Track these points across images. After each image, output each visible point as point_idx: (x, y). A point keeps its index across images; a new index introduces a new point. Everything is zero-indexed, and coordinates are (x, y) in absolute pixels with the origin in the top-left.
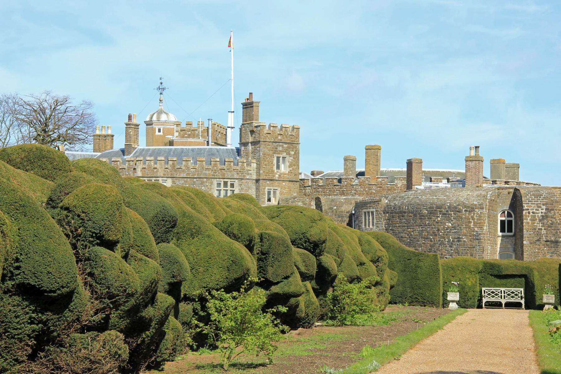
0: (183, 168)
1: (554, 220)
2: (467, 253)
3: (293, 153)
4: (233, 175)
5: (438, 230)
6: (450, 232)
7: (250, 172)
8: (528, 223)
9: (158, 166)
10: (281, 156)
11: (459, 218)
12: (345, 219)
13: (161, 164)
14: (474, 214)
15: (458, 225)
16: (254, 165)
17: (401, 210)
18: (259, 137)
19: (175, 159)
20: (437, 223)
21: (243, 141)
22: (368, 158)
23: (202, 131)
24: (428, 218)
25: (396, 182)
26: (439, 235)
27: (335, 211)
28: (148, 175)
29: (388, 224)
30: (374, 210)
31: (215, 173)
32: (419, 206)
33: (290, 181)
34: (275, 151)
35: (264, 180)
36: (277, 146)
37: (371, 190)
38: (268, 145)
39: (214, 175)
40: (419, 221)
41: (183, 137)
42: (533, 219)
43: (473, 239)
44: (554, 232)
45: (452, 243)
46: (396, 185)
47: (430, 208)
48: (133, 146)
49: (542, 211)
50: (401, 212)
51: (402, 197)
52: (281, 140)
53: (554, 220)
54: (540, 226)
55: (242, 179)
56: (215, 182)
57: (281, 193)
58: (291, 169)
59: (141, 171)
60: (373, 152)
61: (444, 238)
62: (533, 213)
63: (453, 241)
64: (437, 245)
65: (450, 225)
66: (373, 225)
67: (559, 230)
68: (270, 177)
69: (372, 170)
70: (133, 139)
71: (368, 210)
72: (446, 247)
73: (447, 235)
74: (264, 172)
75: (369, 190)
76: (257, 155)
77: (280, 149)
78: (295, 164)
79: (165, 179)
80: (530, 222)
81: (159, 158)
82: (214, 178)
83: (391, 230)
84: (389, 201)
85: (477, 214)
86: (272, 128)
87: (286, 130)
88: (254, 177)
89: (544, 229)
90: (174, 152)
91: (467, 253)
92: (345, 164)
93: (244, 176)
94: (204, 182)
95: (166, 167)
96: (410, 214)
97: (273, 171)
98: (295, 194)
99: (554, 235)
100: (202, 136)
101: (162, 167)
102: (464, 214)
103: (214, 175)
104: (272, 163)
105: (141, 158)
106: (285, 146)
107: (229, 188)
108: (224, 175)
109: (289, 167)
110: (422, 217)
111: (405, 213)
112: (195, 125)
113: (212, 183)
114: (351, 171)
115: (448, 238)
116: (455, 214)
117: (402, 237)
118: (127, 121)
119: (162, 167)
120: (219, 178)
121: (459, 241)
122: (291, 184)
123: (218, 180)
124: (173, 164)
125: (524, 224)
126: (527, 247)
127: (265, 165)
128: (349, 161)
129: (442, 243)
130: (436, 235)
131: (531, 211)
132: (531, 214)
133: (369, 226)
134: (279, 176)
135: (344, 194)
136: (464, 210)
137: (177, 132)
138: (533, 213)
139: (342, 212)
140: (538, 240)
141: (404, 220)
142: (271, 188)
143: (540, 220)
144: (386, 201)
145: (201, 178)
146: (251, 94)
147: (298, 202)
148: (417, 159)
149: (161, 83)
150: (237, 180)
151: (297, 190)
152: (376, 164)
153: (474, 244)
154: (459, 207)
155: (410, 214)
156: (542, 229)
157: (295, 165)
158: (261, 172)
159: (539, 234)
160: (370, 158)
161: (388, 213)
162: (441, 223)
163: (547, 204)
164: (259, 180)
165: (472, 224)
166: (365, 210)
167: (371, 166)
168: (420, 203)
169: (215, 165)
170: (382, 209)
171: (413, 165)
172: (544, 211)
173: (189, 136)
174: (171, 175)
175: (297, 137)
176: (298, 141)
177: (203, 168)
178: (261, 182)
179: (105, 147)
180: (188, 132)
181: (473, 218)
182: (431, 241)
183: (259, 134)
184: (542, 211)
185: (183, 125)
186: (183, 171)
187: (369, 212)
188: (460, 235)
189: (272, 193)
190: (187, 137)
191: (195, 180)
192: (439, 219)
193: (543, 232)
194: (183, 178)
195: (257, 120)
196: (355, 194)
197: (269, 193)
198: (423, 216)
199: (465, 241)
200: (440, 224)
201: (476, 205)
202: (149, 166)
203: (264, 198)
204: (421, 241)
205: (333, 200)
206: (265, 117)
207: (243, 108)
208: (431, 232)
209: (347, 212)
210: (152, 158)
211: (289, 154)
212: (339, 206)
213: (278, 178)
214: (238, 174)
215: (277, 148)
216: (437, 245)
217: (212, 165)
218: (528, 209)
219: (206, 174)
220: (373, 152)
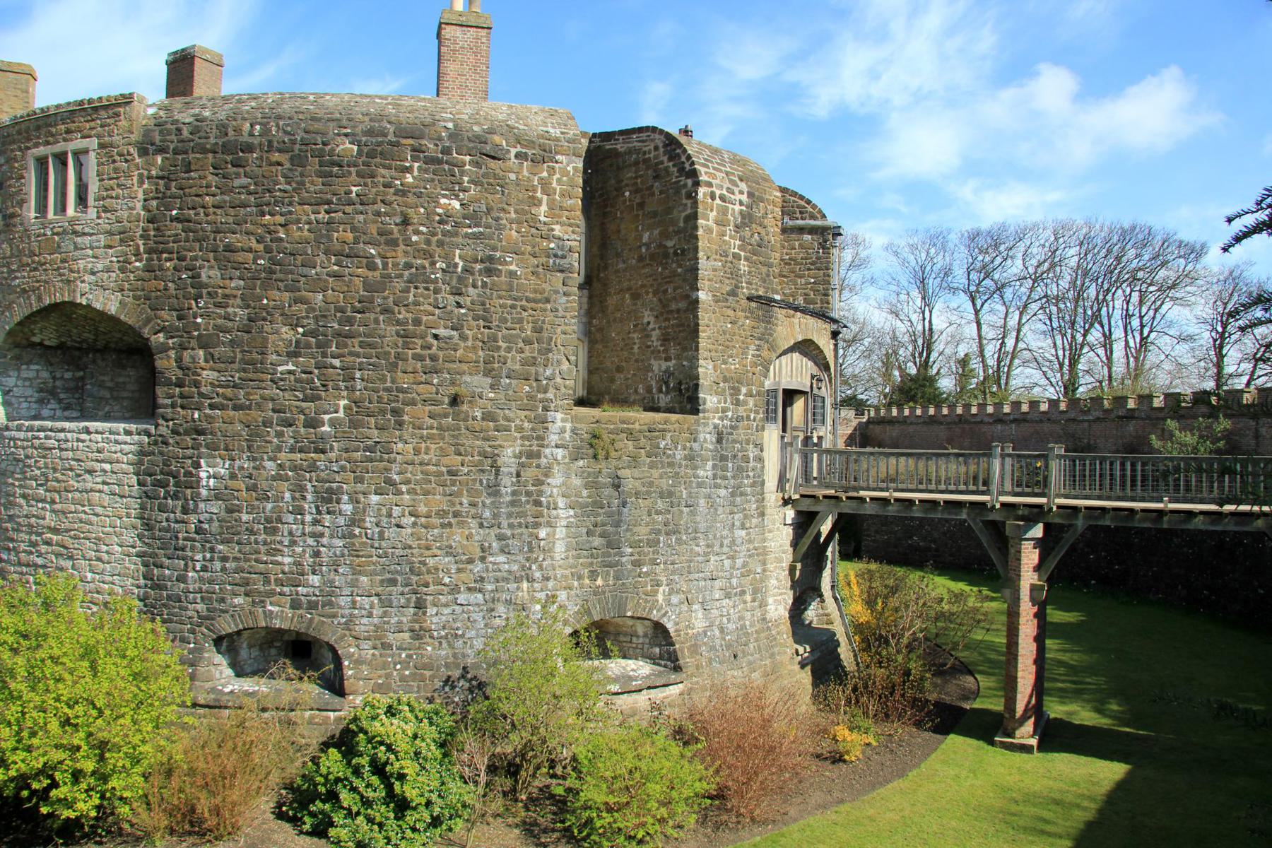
2: (520, 321)
5: (406, 222)
6: (456, 234)
8: (710, 230)
11: (493, 183)
14: (552, 171)
15: (489, 210)
20: (402, 193)
24: (359, 175)
26: (408, 243)
29: (162, 197)
30: (93, 143)
32: (317, 126)
40: (315, 185)
42: (721, 223)
43: (546, 267)
44: (764, 269)
45: (460, 279)
47: (370, 133)
50: (226, 148)
61: (429, 255)
62: (722, 198)
63: (465, 270)
64: (399, 285)
65: (456, 204)
72: (436, 291)
73: (440, 244)
83: (177, 219)
85: (564, 173)
91: (520, 321)
96: (276, 156)
102: (515, 170)
110: (332, 166)
111: (249, 148)
115: (448, 258)
116: (477, 164)
117: (230, 249)
121: (489, 272)
125: (700, 232)
126: (706, 311)
129: (419, 278)
130: (393, 243)
131: (718, 193)
132: (718, 201)
133: (62, 208)
136: (513, 151)
138: (722, 198)
140: (733, 293)
143: (737, 227)
148: (206, 51)
153: (546, 287)
154: (497, 139)
155: (276, 156)
161: (162, 150)
162: (419, 195)
165: (544, 208)
168: (321, 113)
170: (134, 137)
172: (744, 198)
181: (545, 185)
182: (371, 267)
187: (61, 159)
188: (494, 249)
192: (409, 179)
193: (743, 266)
198: (333, 164)
199: (512, 274)
200: (411, 199)
201: (557, 140)
204: (325, 265)
208: (373, 229)
216: (399, 285)
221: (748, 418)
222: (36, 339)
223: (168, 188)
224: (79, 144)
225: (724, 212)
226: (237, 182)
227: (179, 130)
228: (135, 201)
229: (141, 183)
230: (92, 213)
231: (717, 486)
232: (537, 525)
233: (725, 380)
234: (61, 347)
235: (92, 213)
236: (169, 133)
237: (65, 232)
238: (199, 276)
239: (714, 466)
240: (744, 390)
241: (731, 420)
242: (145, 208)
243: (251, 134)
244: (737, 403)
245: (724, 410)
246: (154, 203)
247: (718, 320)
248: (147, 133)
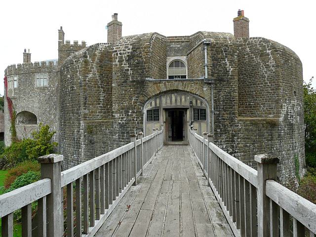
1: (140, 59)
42: (121, 61)
44: (140, 71)
49: (129, 51)
53: (140, 59)
54: (126, 66)
62: (120, 54)
67: (145, 68)
80: (118, 63)
89: (131, 70)
99: (141, 75)
118: (24, 52)
132: (119, 55)
138: (120, 54)
140: (125, 82)
156: (128, 70)
159: (125, 74)
163: (134, 44)
184: (129, 51)
218: (116, 51)
221: (133, 120)
225: (121, 57)
231: (121, 141)
232: (79, 149)
233: (122, 109)
239: (119, 135)
240: (130, 111)
241: (125, 121)
244: (128, 115)
245: (122, 118)
247: (119, 91)
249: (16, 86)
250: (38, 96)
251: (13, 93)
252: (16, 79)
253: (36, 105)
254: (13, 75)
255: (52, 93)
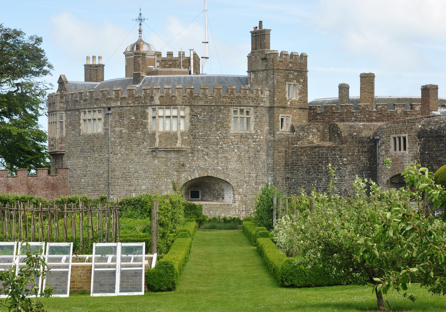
0: (201, 96)
3: (302, 80)
4: (248, 103)
7: (264, 100)
9: (176, 94)
10: (292, 83)
12: (366, 144)
13: (179, 92)
16: (267, 93)
17: (439, 134)
18: (273, 65)
19: (193, 87)
21: (254, 69)
22: (363, 86)
23: (183, 62)
25: (396, 109)
27: (355, 137)
28: (166, 103)
31: (232, 100)
33: (300, 108)
34: (287, 79)
35: (278, 107)
36: (289, 73)
37: (372, 116)
38: (281, 73)
39: (231, 103)
41: (164, 67)
46: (396, 112)
48: (142, 75)
51: (437, 122)
52: (291, 68)
55: (257, 107)
56: (232, 109)
57: (293, 121)
58: (301, 96)
59: (159, 99)
60: (367, 80)
66: (405, 149)
68: (283, 105)
69: (367, 97)
70: (141, 68)
71: (399, 135)
74: (278, 99)
75: (370, 117)
76: (271, 82)
77: (291, 76)
78: (304, 92)
79: (183, 107)
81: (177, 87)
82: (231, 106)
83: (427, 154)
84: (423, 125)
86: (284, 56)
87: (296, 58)
88: (268, 105)
90: (184, 81)
92: (340, 92)
93: (259, 104)
94: (221, 110)
95: (184, 95)
97: (285, 99)
98: (305, 121)
100: (183, 66)
101: (180, 95)
103: (231, 103)
104: (284, 91)
105: (159, 87)
106: (296, 74)
107: (245, 115)
108: (240, 102)
109: (299, 95)
111: (443, 137)
112: (176, 55)
113: (229, 111)
114: (346, 98)
119: (180, 95)
120: (236, 106)
122: (301, 112)
123: (235, 107)
124: (191, 92)
127: (279, 92)
128: (344, 89)
133: (400, 150)
134: (291, 103)
135: (344, 121)
137: (158, 62)
139: (363, 138)
141: (442, 145)
142: (284, 115)
144: (420, 126)
145: (219, 106)
146: (261, 22)
147: (313, 129)
149: (140, 14)
150: (252, 108)
151: (306, 117)
152: (371, 91)
157: (304, 93)
158: (275, 99)
160: (365, 86)
164: (274, 107)
166: (395, 136)
167: (366, 93)
169: (232, 93)
171: (430, 91)
173: (170, 66)
174: (189, 103)
175: (305, 64)
176: (307, 69)
177: (220, 96)
178: (275, 109)
179: (97, 77)
180: (170, 62)
183: (273, 61)
185: (164, 55)
186: (201, 99)
187: (400, 138)
189: (284, 120)
190: (168, 67)
191: (213, 108)
194: (201, 105)
195: (269, 48)
196: (355, 121)
197: (282, 120)
202: (168, 94)
203: (279, 125)
205: (351, 127)
206: (277, 45)
207: (252, 36)
209: (367, 138)
210: (170, 86)
211: (298, 81)
212: (359, 132)
213: (290, 105)
214: (253, 101)
215: (288, 76)
217: (229, 93)
219: (223, 102)
220: (367, 80)
222: (394, 182)
223: (425, 146)
224: (403, 135)
226: (441, 145)
227: (427, 132)
228: (417, 149)
229: (419, 145)
230: (407, 152)
234: (399, 183)
235: (407, 152)
236: (425, 133)
237: (401, 156)
238: (433, 167)
242: (420, 151)
243: (443, 133)
246: (422, 150)
248: (419, 133)
249: (182, 128)
250: (236, 150)
251: (179, 141)
252: (182, 113)
253: (233, 165)
254: (179, 107)
255: (260, 145)
